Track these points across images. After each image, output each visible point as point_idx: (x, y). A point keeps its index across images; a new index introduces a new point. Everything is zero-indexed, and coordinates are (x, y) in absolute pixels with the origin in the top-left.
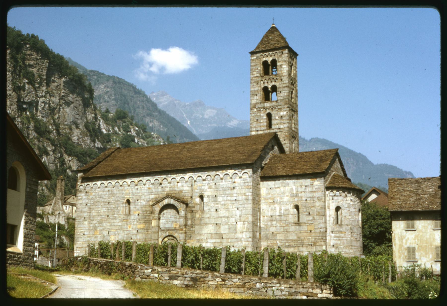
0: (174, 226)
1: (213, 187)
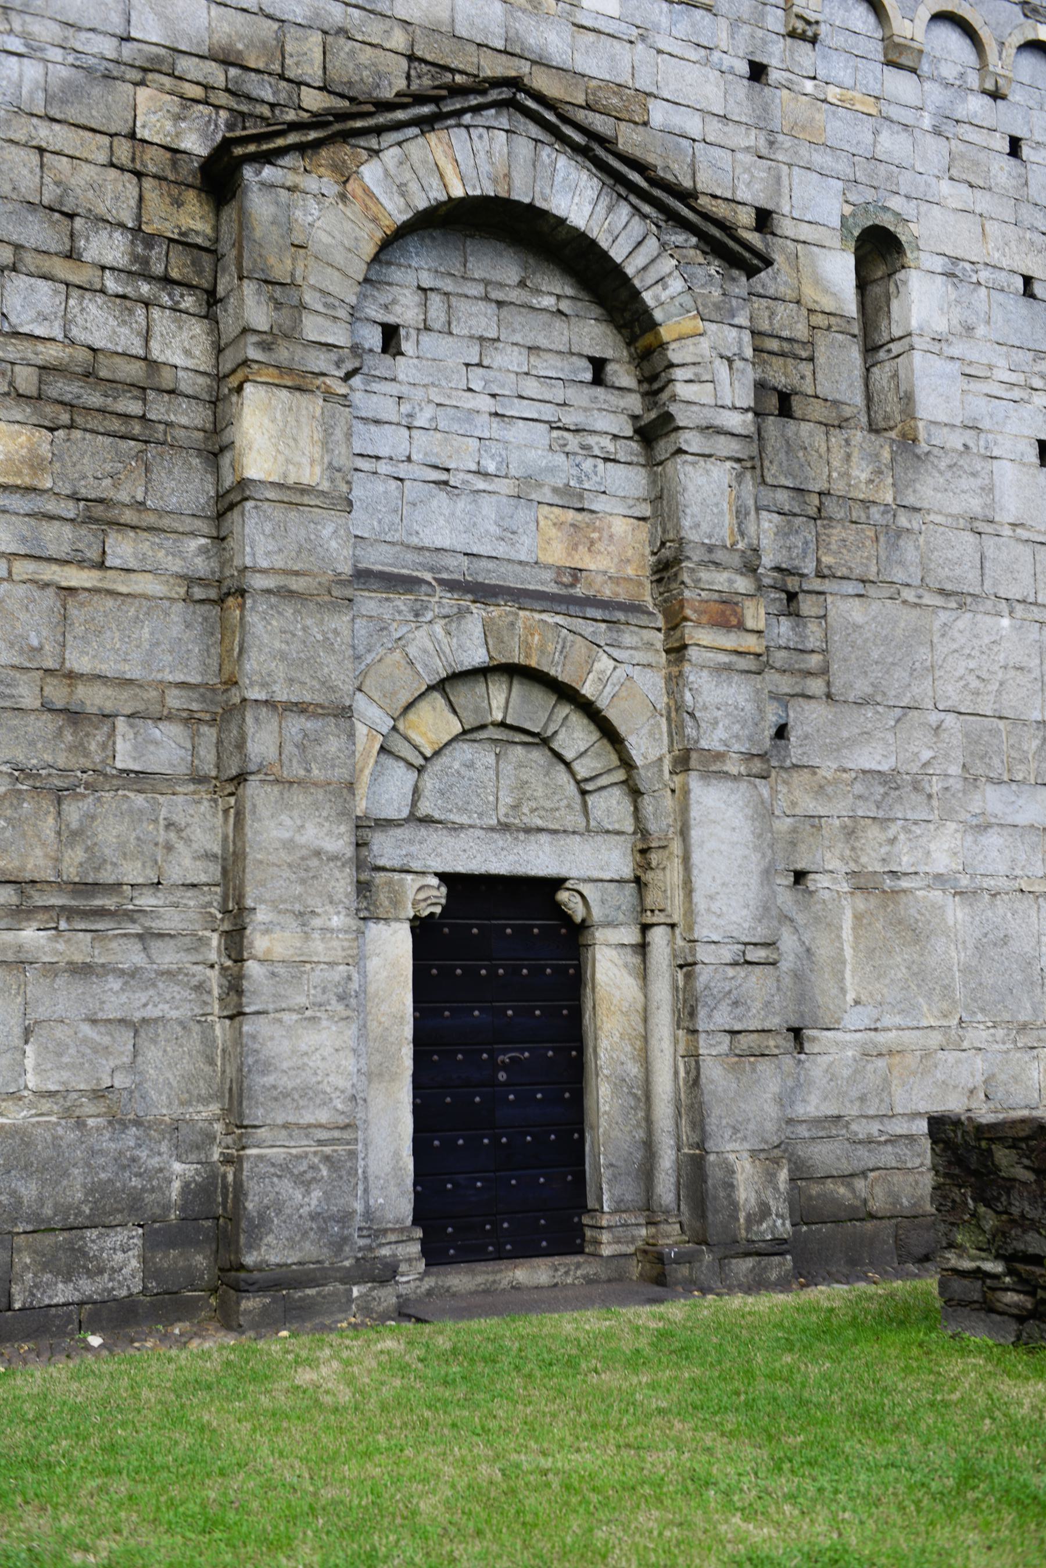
0: (557, 554)
1: (1002, 168)
